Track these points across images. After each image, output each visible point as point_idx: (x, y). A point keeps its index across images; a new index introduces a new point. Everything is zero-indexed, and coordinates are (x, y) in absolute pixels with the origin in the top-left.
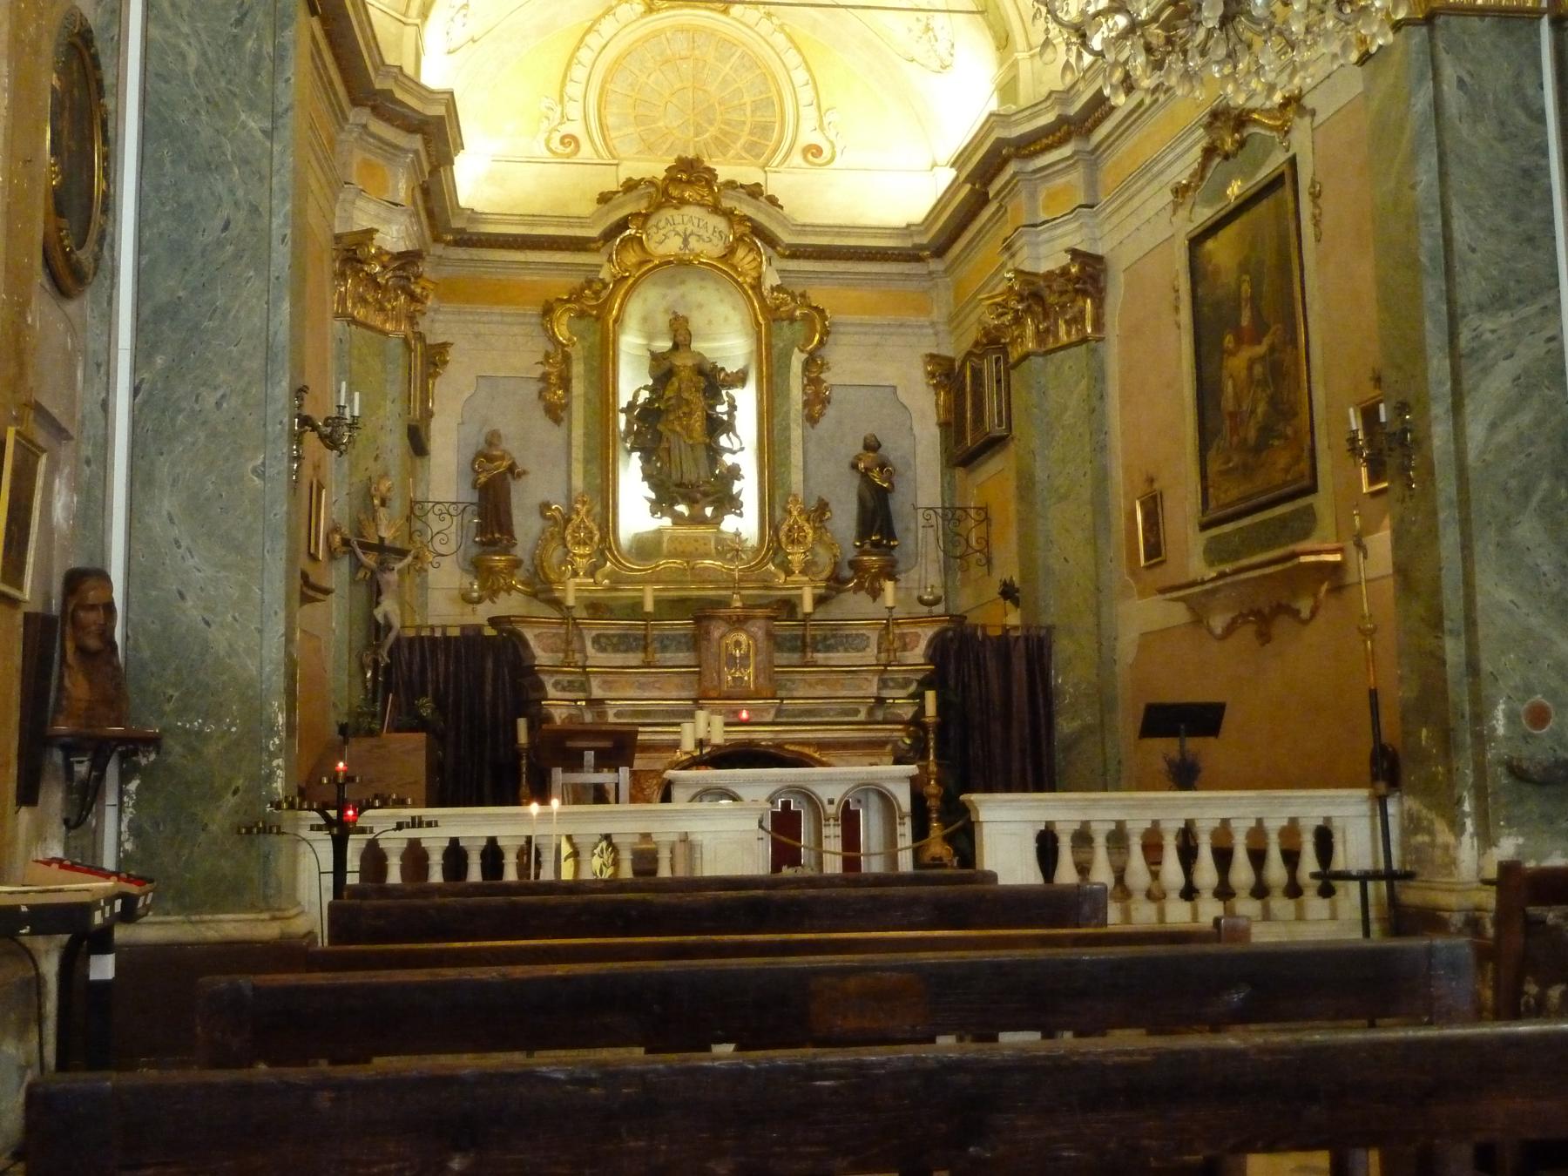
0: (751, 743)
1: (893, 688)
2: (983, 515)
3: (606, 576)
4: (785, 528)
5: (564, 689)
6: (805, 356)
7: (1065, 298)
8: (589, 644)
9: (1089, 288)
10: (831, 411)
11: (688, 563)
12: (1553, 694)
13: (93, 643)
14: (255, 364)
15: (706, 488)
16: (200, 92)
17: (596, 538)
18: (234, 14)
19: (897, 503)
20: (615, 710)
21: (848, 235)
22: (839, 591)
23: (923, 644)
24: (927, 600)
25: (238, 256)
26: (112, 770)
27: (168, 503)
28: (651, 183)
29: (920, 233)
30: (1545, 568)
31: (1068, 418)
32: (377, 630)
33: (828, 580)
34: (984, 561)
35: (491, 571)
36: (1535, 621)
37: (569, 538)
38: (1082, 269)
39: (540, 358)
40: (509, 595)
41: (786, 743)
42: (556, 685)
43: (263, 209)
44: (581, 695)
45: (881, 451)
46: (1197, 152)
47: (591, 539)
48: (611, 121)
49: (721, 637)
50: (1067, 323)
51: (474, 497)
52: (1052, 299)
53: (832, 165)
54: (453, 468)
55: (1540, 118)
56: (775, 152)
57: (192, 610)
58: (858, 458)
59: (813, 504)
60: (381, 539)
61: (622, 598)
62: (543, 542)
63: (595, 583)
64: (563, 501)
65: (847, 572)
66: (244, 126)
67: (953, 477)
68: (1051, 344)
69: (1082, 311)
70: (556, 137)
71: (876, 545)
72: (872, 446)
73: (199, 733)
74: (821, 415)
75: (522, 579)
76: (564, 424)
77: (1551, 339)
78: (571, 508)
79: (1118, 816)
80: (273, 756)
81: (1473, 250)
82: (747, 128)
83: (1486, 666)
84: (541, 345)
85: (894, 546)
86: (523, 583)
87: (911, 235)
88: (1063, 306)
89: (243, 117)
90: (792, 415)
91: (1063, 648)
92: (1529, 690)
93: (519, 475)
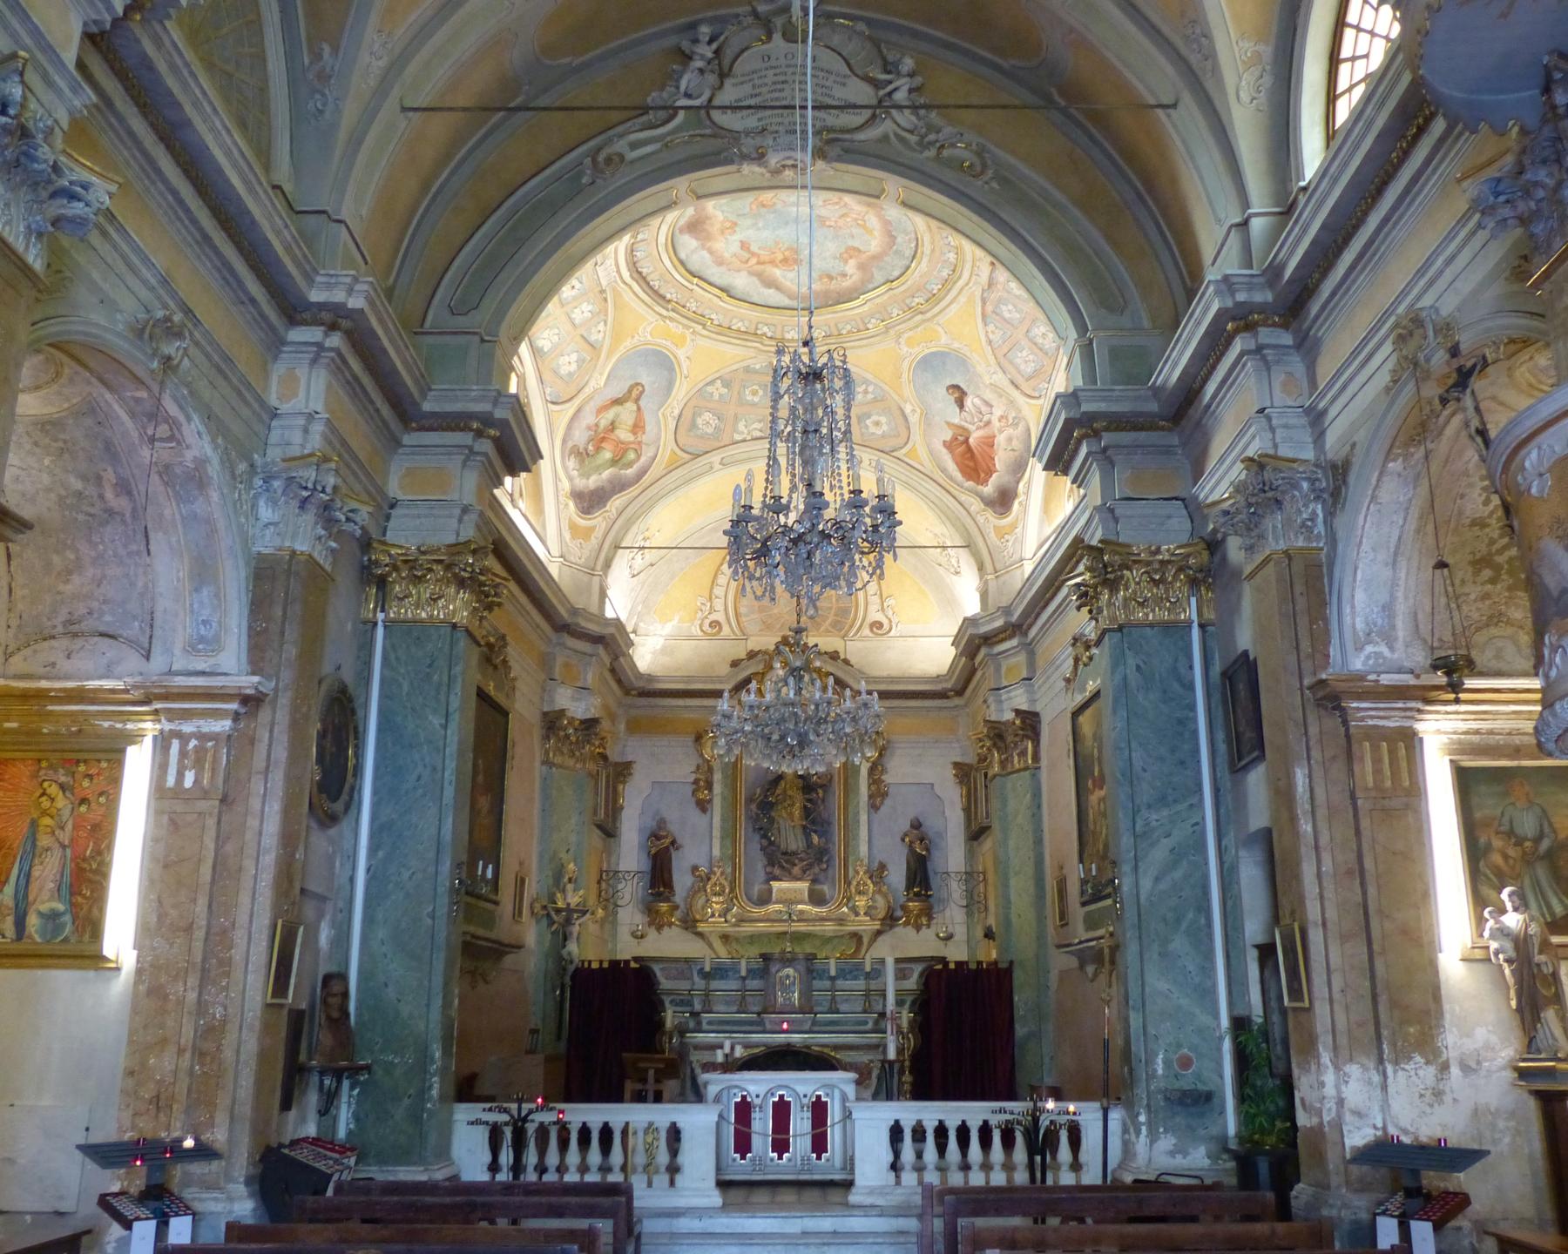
0: (789, 1045)
3: (734, 916)
4: (854, 883)
6: (869, 765)
7: (1017, 739)
9: (1029, 733)
10: (888, 802)
12: (1193, 1048)
13: (335, 1014)
14: (431, 855)
15: (802, 855)
16: (409, 705)
18: (428, 661)
19: (936, 864)
21: (898, 683)
22: (892, 927)
23: (916, 975)
25: (424, 795)
26: (346, 1084)
27: (381, 933)
28: (765, 652)
29: (946, 681)
30: (1191, 968)
31: (1020, 820)
32: (561, 962)
33: (883, 919)
35: (657, 912)
36: (1184, 1002)
38: (1023, 722)
39: (693, 768)
42: (671, 1002)
43: (440, 767)
44: (688, 1009)
45: (923, 829)
46: (1071, 661)
48: (743, 610)
49: (778, 971)
50: (1019, 755)
51: (645, 865)
52: (1010, 739)
53: (892, 634)
54: (636, 843)
55: (1191, 687)
56: (851, 626)
57: (391, 993)
58: (906, 835)
59: (876, 864)
60: (569, 904)
62: (694, 892)
63: (726, 921)
64: (707, 865)
65: (899, 913)
66: (431, 723)
67: (971, 846)
68: (1009, 770)
69: (1027, 748)
70: (707, 622)
71: (916, 894)
72: (917, 825)
73: (392, 1063)
74: (882, 803)
76: (709, 813)
77: (1197, 824)
78: (711, 868)
79: (942, 1118)
80: (433, 1075)
81: (1145, 770)
82: (833, 612)
83: (1152, 1031)
84: (695, 760)
86: (680, 920)
87: (941, 682)
88: (1016, 744)
89: (430, 717)
90: (861, 804)
91: (1018, 977)
92: (1179, 1046)
93: (677, 849)
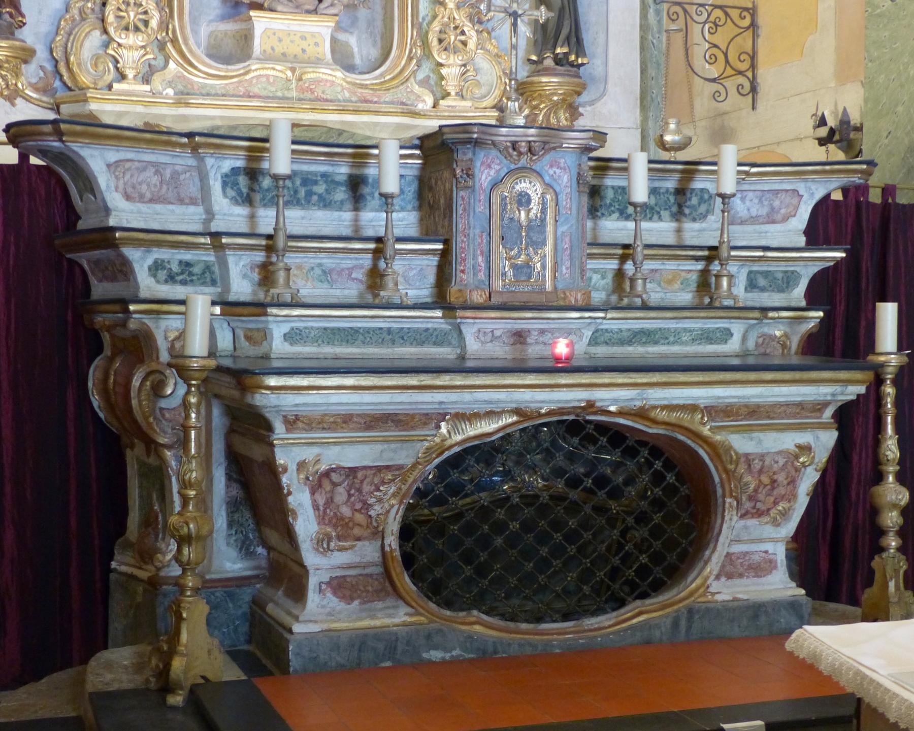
1: (763, 289)
2: (747, 22)
3: (170, 84)
5: (171, 278)
8: (216, 186)
11: (293, 70)
17: (154, 23)
20: (285, 328)
24: (674, 142)
34: (747, 85)
37: (111, 18)
40: (13, 105)
41: (655, 407)
47: (146, 23)
61: (199, 118)
75: (34, 81)
85: (583, 64)
86: (36, 89)
